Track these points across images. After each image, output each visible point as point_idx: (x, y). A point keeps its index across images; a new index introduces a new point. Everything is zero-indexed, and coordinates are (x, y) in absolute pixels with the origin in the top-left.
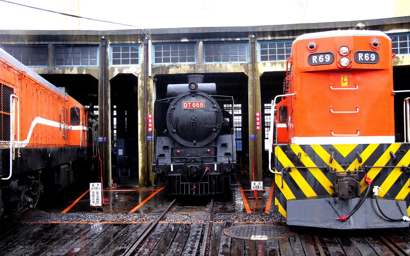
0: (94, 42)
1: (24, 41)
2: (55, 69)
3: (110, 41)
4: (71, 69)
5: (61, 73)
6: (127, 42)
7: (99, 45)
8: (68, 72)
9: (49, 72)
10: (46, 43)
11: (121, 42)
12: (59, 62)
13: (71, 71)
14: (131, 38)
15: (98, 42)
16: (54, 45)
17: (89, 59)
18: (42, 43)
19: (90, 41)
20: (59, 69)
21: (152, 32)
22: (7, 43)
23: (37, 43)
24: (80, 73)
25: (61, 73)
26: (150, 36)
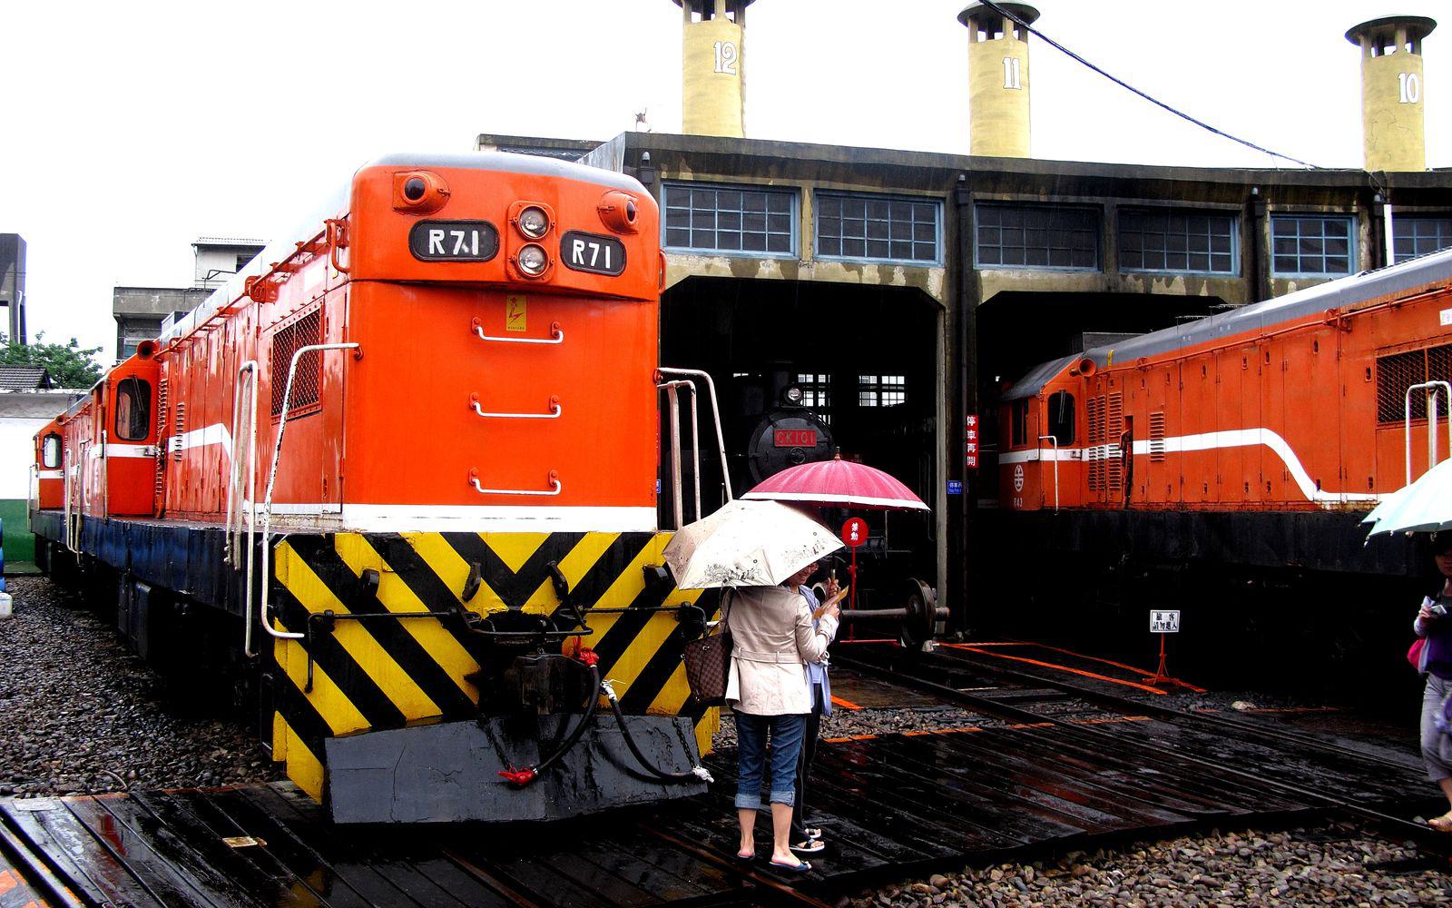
0: (1229, 205)
1: (1038, 193)
2: (1124, 277)
3: (1272, 203)
4: (1170, 281)
5: (1142, 292)
6: (1320, 207)
7: (1240, 211)
8: (1159, 289)
9: (1109, 288)
10: (1098, 200)
11: (1302, 207)
12: (1129, 257)
13: (1168, 286)
14: (1332, 196)
15: (1238, 205)
16: (1118, 206)
17: (1210, 253)
18: (1085, 199)
19: (1217, 201)
20: (1136, 278)
21: (1395, 183)
22: (989, 196)
23: (1072, 199)
24: (1191, 293)
25: (1141, 291)
26: (1389, 192)
